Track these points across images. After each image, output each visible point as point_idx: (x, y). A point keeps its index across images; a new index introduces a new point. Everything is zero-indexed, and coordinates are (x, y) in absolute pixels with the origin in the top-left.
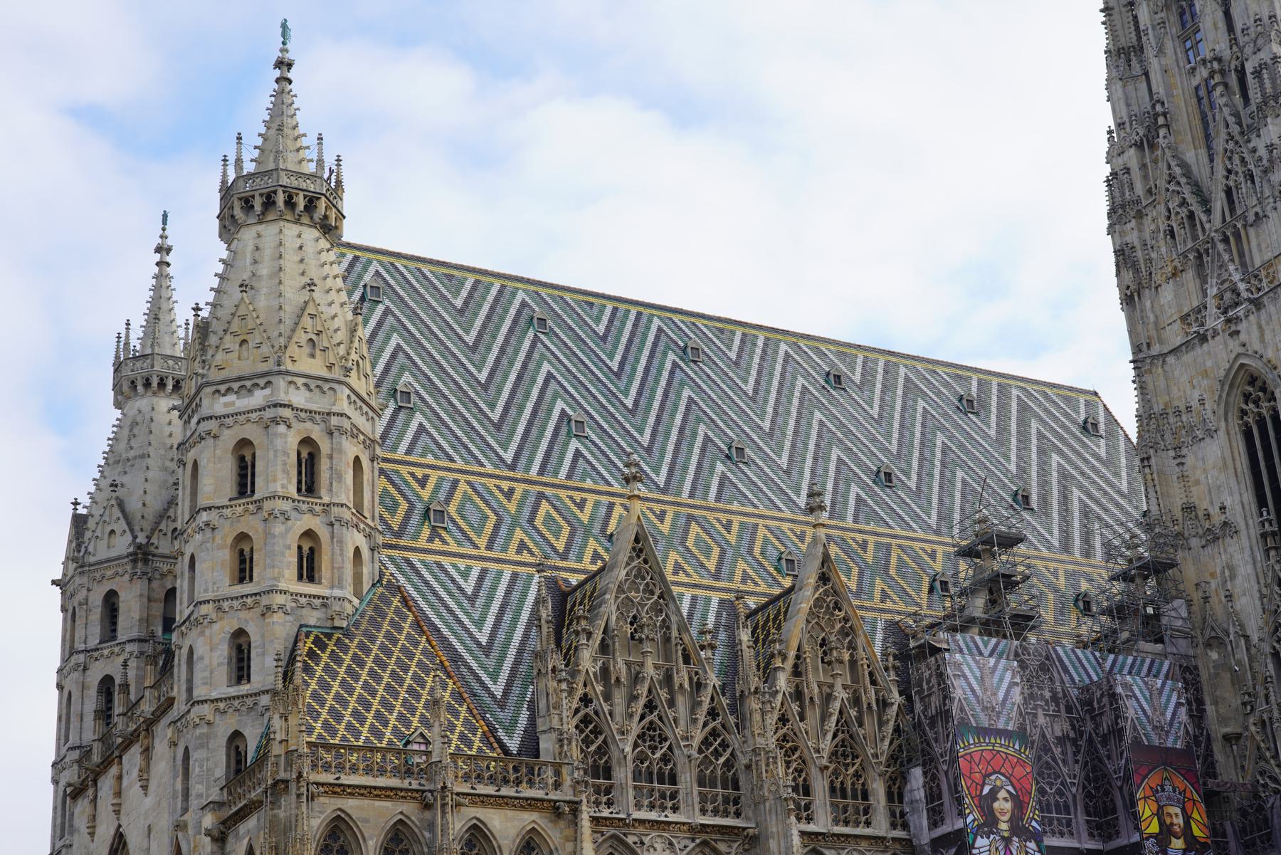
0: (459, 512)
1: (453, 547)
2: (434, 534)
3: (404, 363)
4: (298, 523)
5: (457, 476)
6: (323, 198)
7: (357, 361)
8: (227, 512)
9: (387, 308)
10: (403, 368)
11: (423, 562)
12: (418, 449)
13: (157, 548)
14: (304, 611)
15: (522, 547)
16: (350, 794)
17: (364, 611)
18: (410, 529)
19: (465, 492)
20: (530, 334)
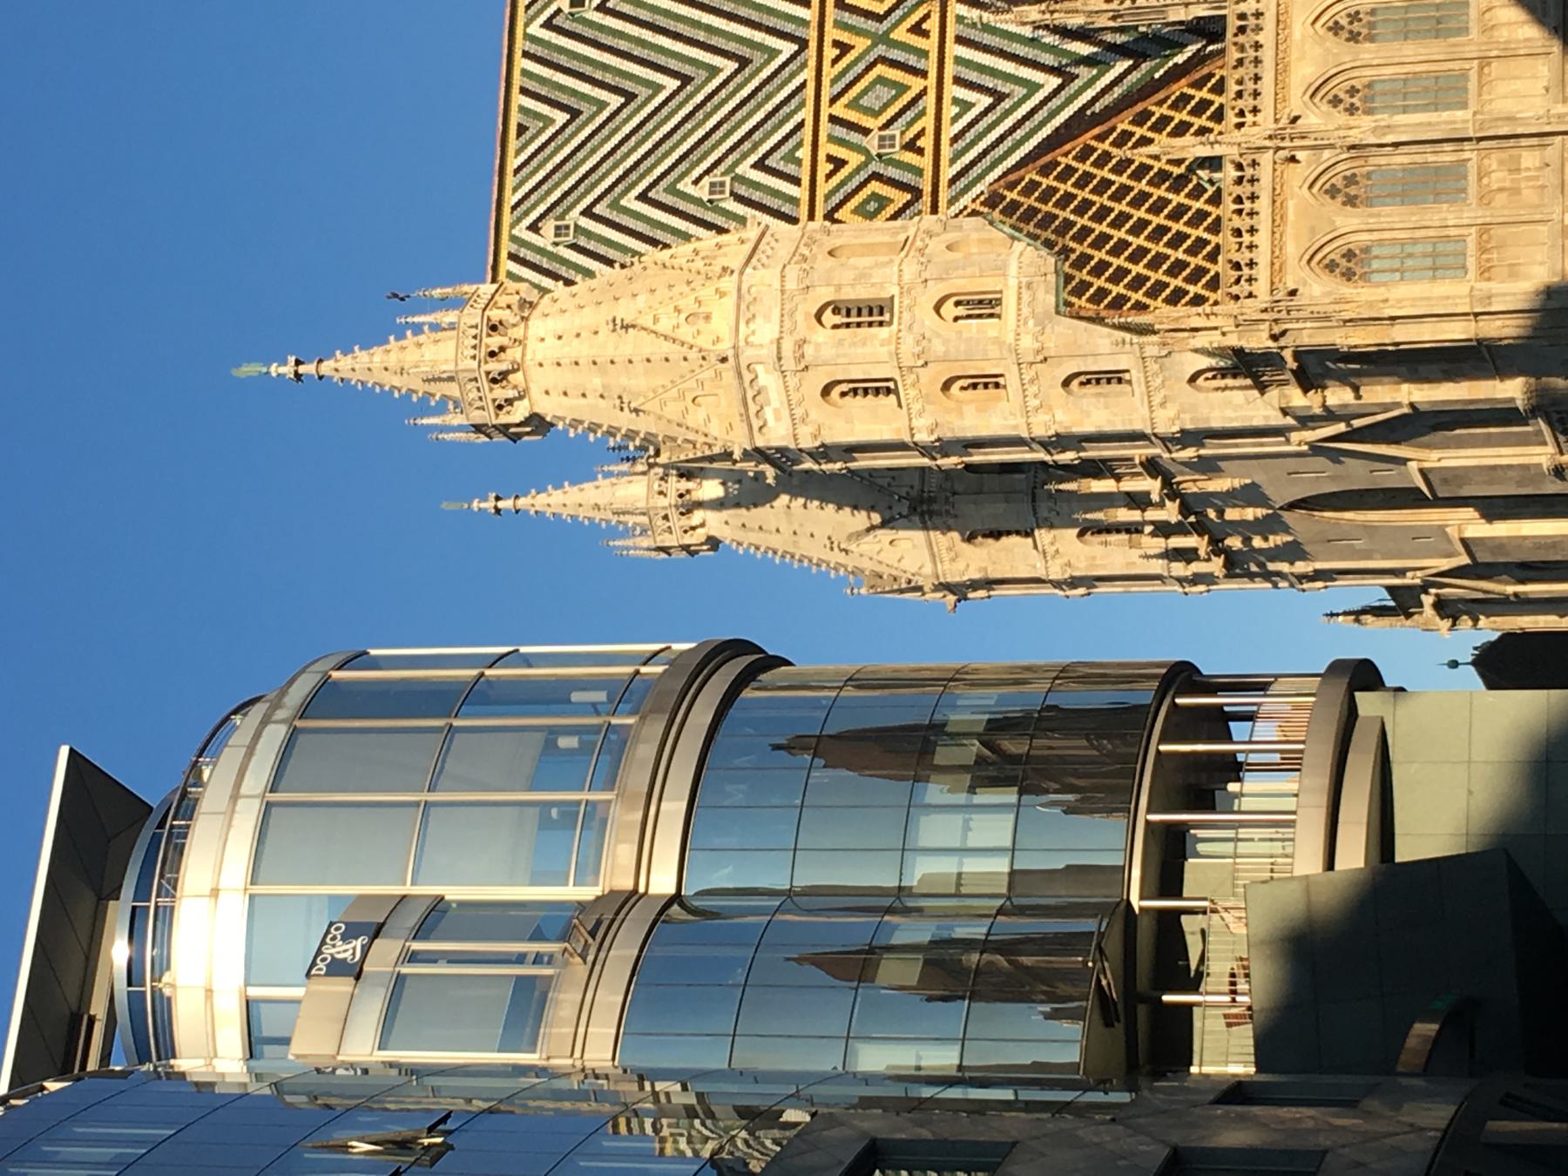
0: (876, 114)
1: (928, 122)
2: (911, 146)
3: (665, 190)
4: (927, 323)
5: (824, 118)
6: (487, 313)
7: (703, 258)
8: (916, 407)
9: (584, 213)
10: (672, 190)
11: (952, 161)
12: (790, 169)
13: (912, 487)
14: (1039, 310)
15: (917, 29)
16: (1281, 249)
17: (1029, 235)
18: (907, 177)
19: (846, 106)
20: (598, 17)
